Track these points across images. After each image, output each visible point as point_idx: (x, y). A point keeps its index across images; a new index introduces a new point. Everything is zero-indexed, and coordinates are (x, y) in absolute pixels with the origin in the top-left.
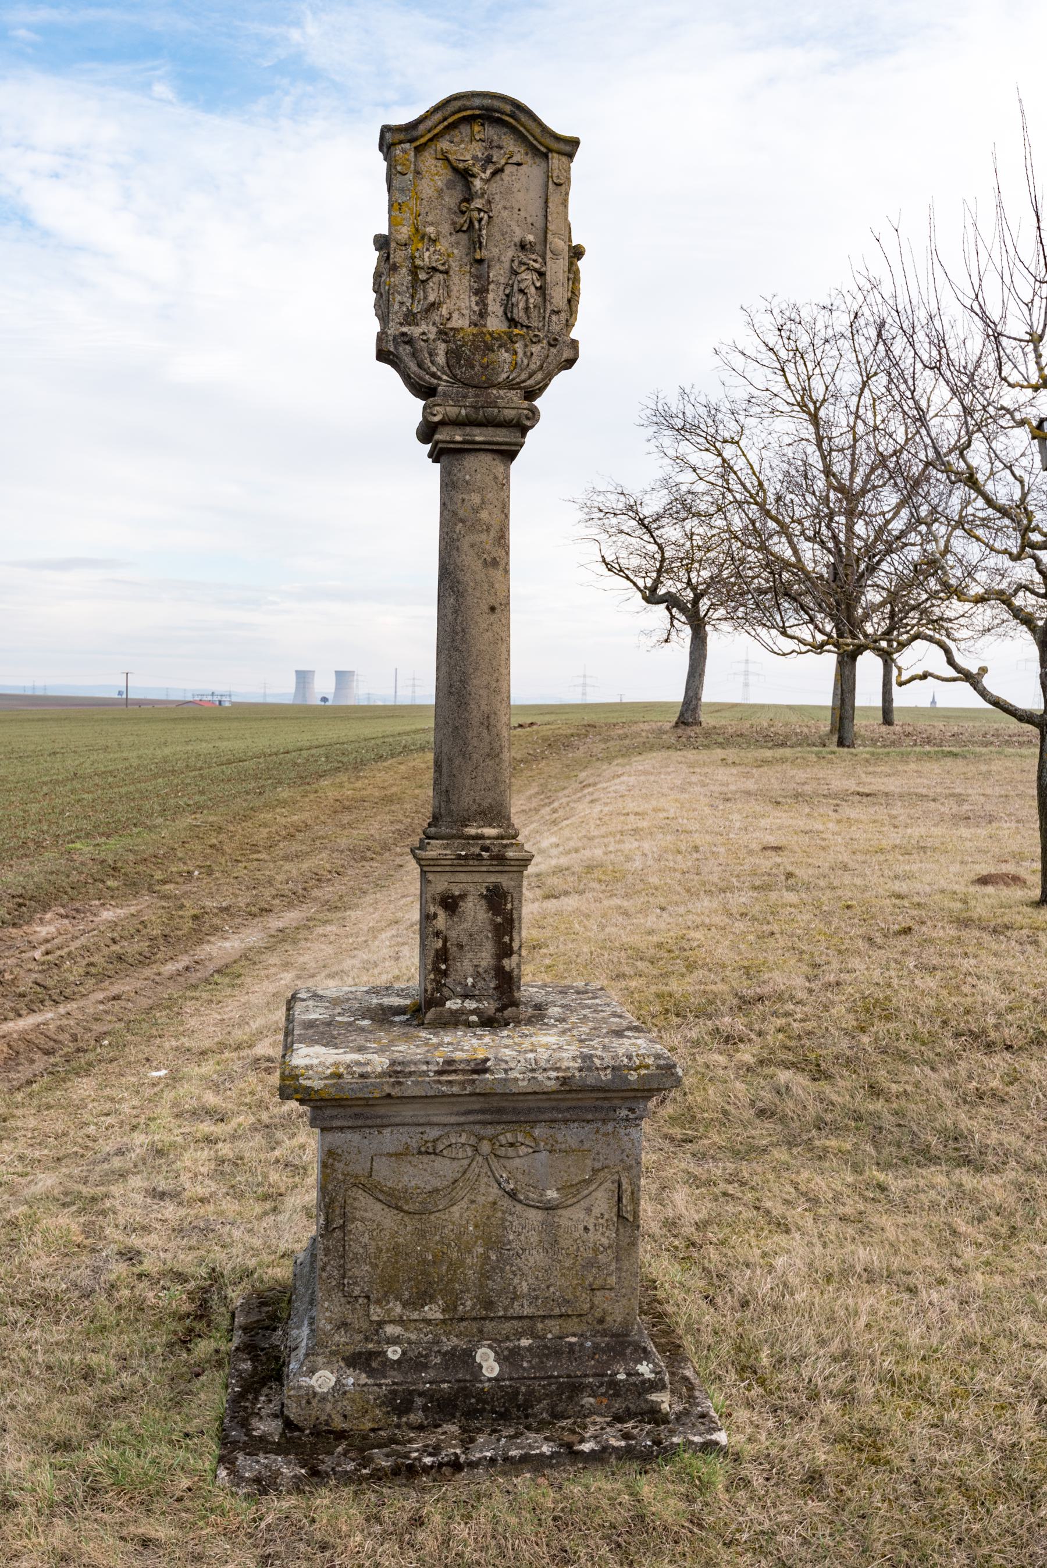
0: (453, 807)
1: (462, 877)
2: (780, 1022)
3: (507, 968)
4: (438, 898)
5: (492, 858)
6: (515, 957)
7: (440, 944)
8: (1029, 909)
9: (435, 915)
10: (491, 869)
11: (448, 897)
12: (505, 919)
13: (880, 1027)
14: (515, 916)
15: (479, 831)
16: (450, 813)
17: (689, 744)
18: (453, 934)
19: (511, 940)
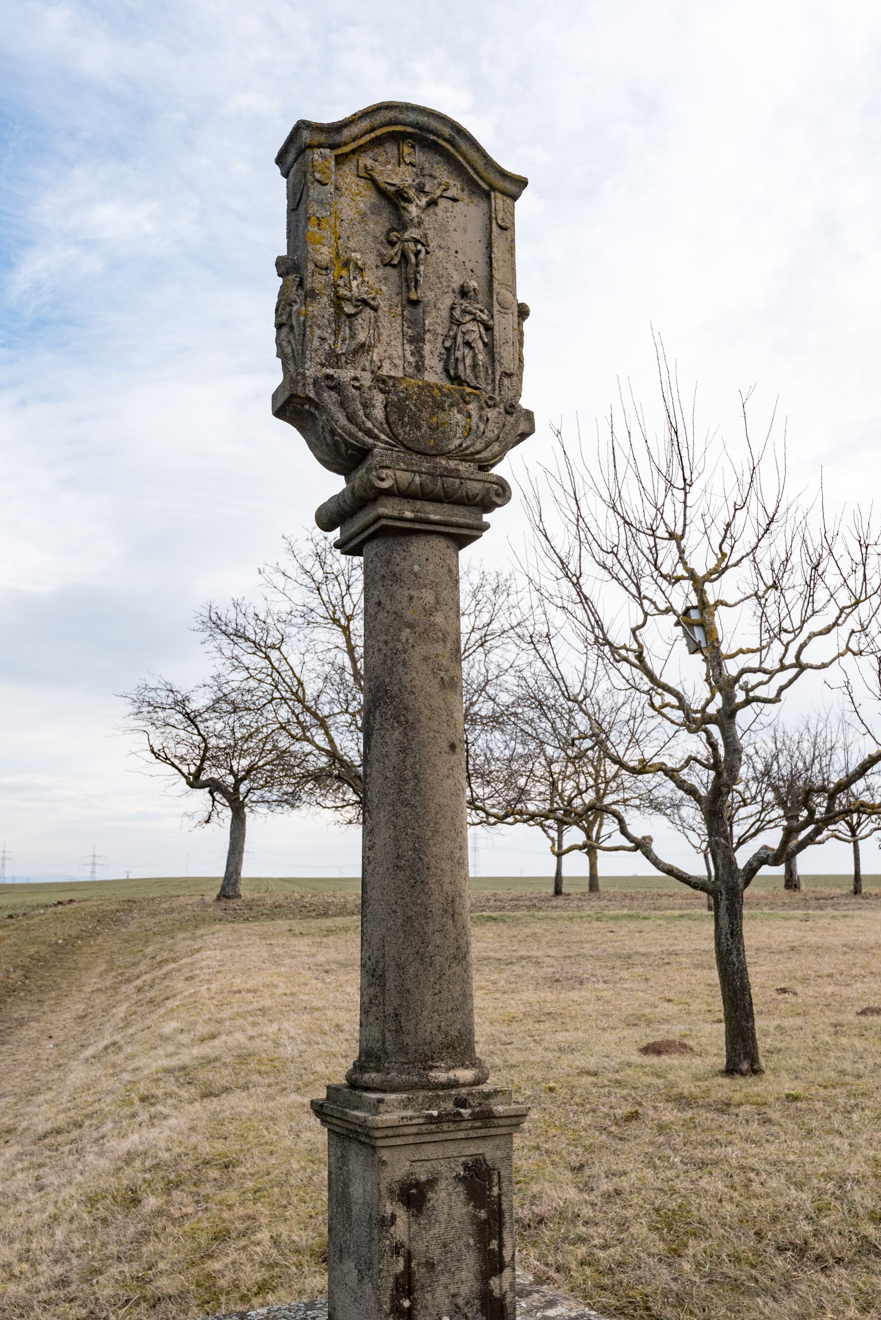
0: (407, 1039)
1: (430, 1151)
2: (582, 1251)
3: (497, 1293)
4: (396, 1187)
5: (475, 1117)
6: (507, 1272)
7: (401, 1266)
8: (721, 1080)
9: (393, 1217)
10: (472, 1134)
11: (411, 1186)
12: (491, 1213)
13: (694, 1247)
14: (505, 1206)
15: (451, 1074)
16: (403, 1049)
17: (237, 917)
18: (419, 1247)
19: (501, 1246)
